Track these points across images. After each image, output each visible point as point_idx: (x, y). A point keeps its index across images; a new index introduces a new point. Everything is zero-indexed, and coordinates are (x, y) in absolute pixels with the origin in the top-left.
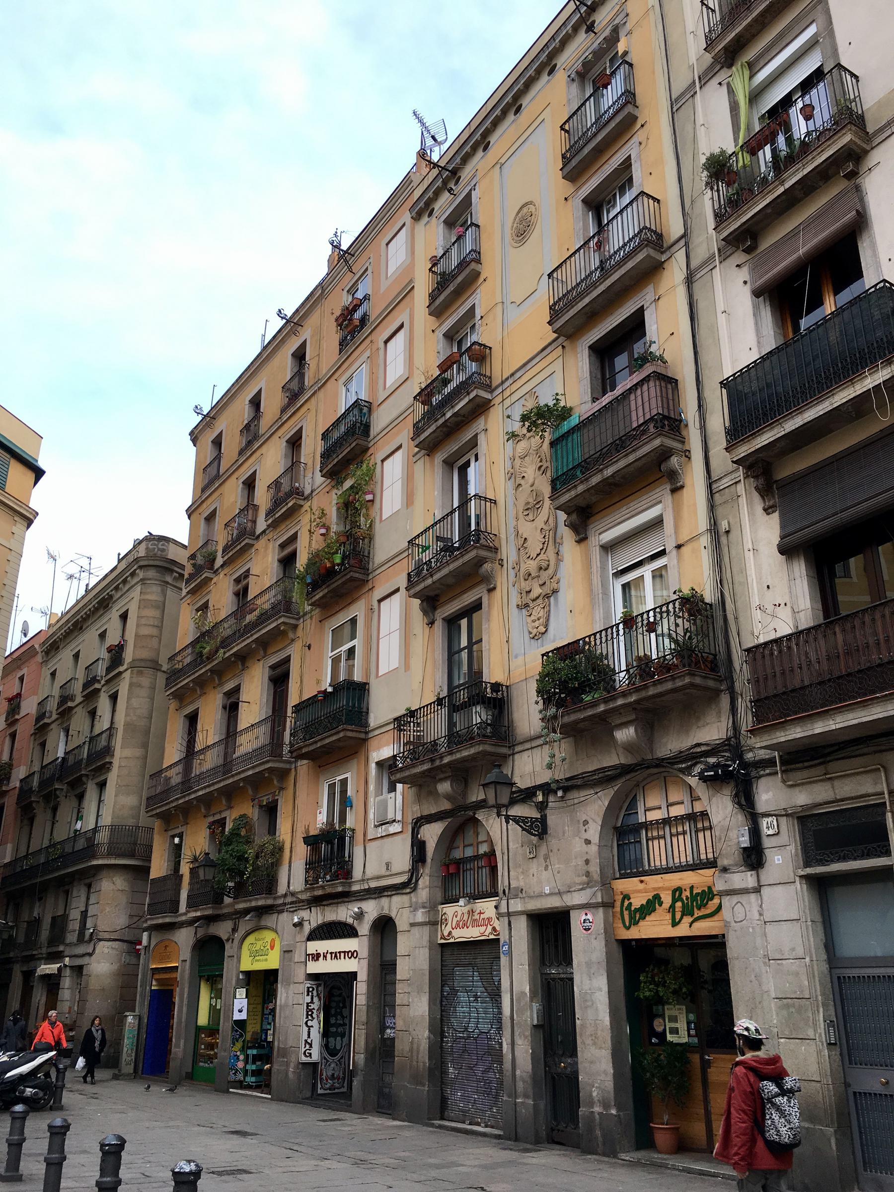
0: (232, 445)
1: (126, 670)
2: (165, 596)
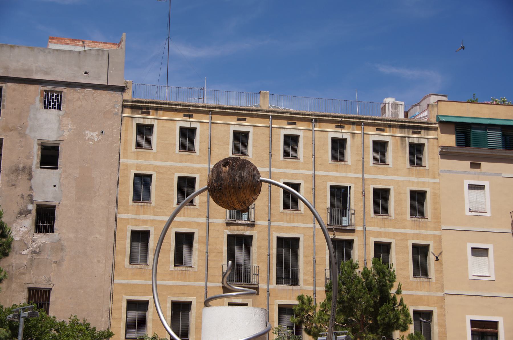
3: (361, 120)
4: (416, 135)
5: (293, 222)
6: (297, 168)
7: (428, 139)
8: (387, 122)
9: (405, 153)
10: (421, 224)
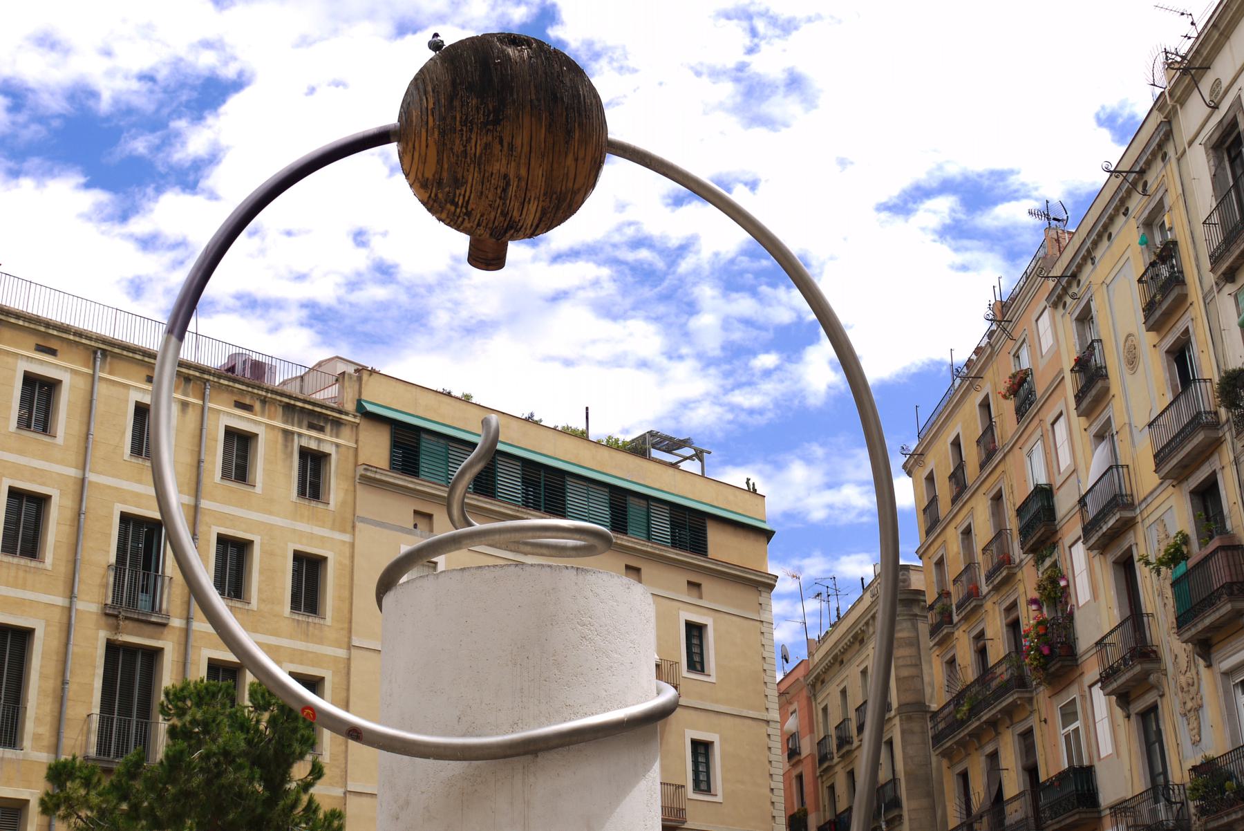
0: (944, 490)
1: (895, 716)
2: (916, 630)
3: (206, 377)
4: (314, 433)
5: (24, 587)
6: (47, 459)
7: (337, 445)
8: (260, 392)
9: (291, 467)
10: (311, 629)
